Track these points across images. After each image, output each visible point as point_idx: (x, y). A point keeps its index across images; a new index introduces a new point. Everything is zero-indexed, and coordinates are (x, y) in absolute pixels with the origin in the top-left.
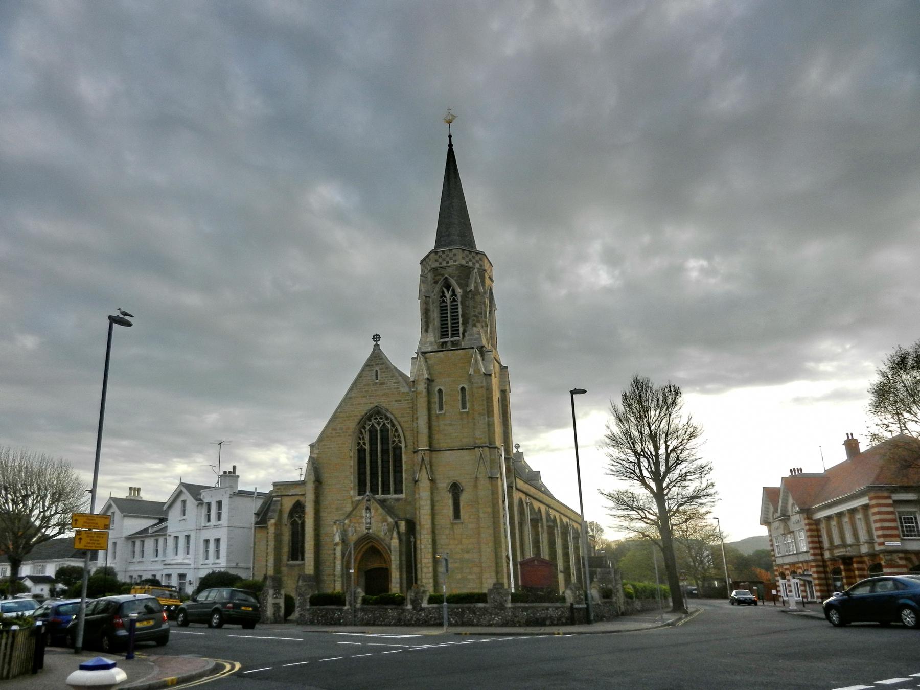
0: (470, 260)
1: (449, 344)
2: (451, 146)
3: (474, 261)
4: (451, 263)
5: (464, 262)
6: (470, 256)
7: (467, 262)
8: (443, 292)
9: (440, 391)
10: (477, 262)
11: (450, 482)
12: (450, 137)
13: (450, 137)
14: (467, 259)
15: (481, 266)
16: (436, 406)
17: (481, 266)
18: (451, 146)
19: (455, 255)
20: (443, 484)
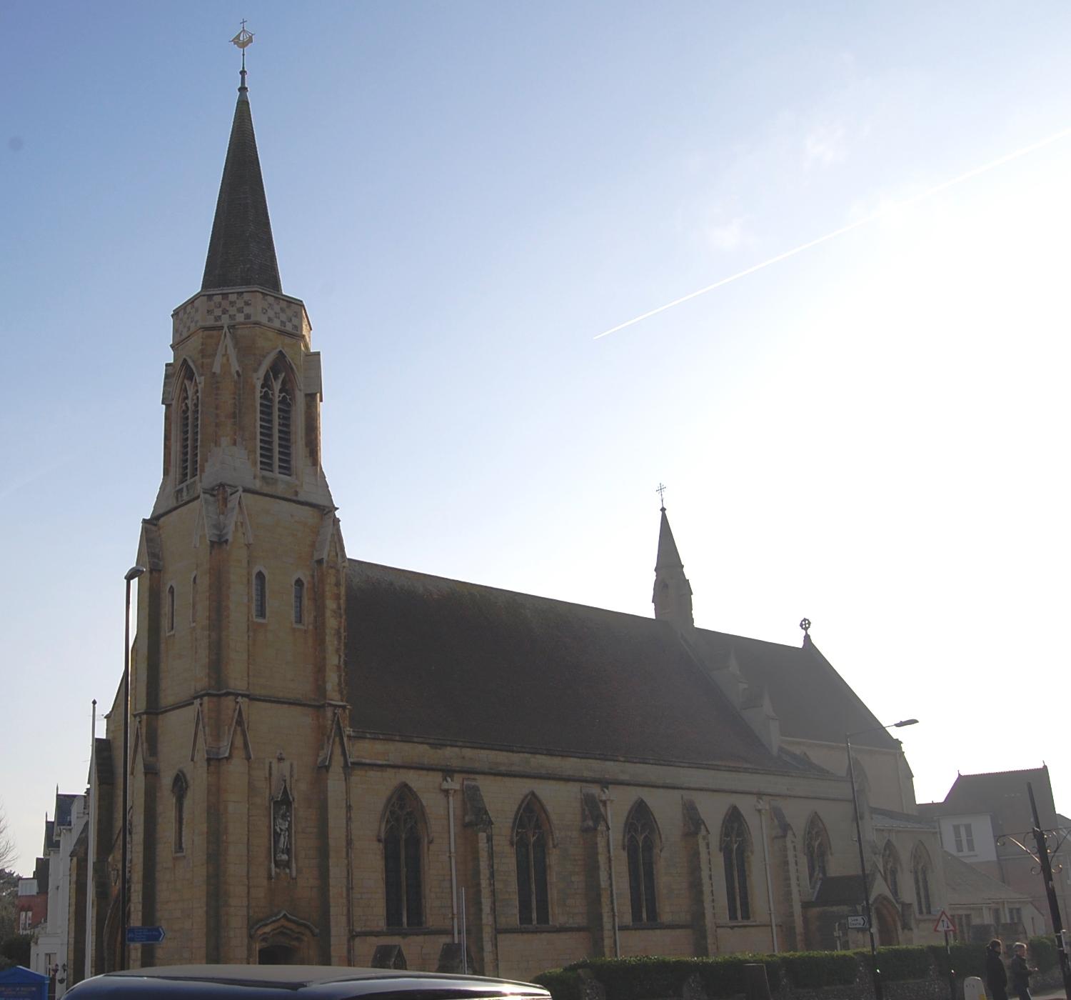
0: (225, 312)
1: (185, 493)
2: (243, 89)
3: (232, 311)
4: (192, 329)
5: (210, 322)
6: (225, 304)
7: (218, 318)
8: (186, 390)
9: (172, 590)
10: (240, 310)
11: (173, 773)
12: (243, 73)
13: (243, 73)
14: (218, 312)
15: (248, 317)
16: (165, 623)
17: (248, 317)
18: (243, 89)
19: (197, 311)
20: (167, 780)
